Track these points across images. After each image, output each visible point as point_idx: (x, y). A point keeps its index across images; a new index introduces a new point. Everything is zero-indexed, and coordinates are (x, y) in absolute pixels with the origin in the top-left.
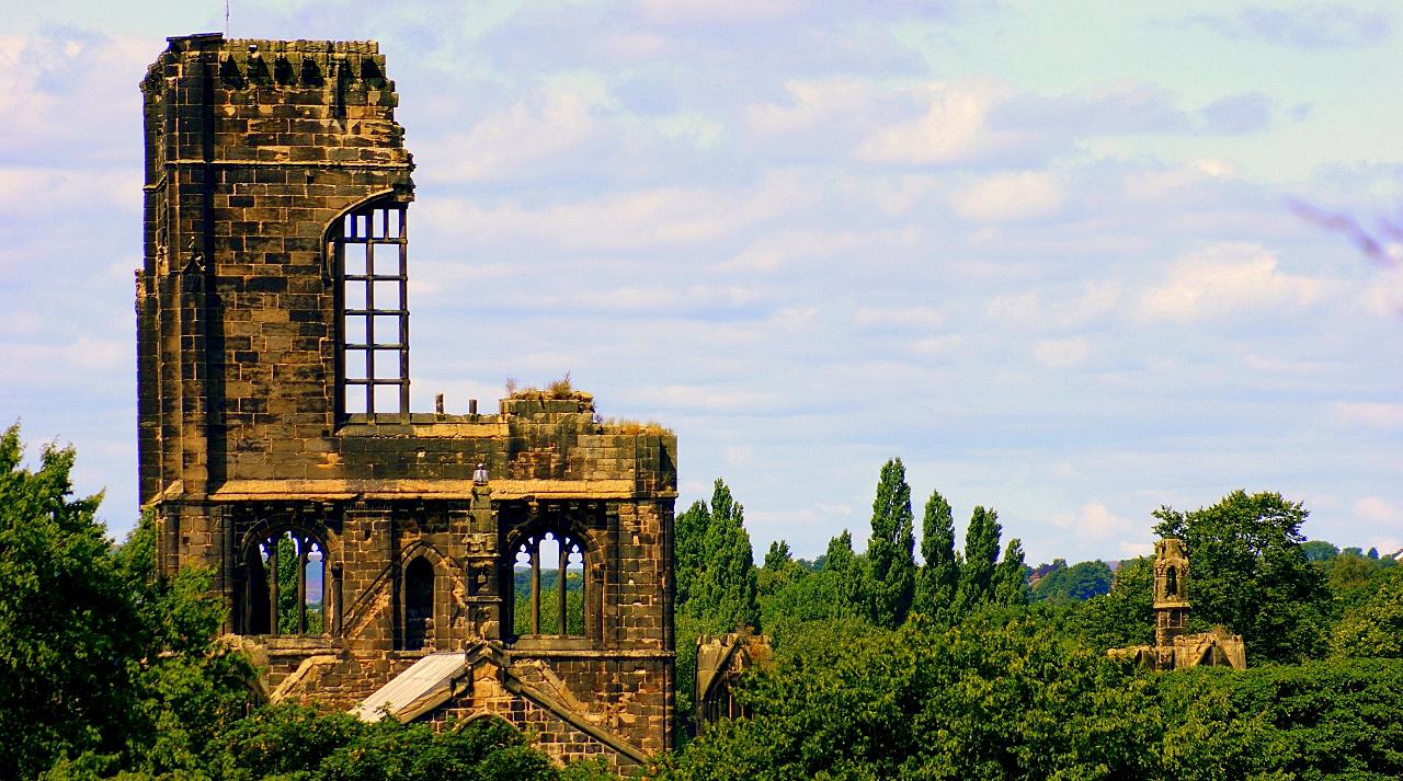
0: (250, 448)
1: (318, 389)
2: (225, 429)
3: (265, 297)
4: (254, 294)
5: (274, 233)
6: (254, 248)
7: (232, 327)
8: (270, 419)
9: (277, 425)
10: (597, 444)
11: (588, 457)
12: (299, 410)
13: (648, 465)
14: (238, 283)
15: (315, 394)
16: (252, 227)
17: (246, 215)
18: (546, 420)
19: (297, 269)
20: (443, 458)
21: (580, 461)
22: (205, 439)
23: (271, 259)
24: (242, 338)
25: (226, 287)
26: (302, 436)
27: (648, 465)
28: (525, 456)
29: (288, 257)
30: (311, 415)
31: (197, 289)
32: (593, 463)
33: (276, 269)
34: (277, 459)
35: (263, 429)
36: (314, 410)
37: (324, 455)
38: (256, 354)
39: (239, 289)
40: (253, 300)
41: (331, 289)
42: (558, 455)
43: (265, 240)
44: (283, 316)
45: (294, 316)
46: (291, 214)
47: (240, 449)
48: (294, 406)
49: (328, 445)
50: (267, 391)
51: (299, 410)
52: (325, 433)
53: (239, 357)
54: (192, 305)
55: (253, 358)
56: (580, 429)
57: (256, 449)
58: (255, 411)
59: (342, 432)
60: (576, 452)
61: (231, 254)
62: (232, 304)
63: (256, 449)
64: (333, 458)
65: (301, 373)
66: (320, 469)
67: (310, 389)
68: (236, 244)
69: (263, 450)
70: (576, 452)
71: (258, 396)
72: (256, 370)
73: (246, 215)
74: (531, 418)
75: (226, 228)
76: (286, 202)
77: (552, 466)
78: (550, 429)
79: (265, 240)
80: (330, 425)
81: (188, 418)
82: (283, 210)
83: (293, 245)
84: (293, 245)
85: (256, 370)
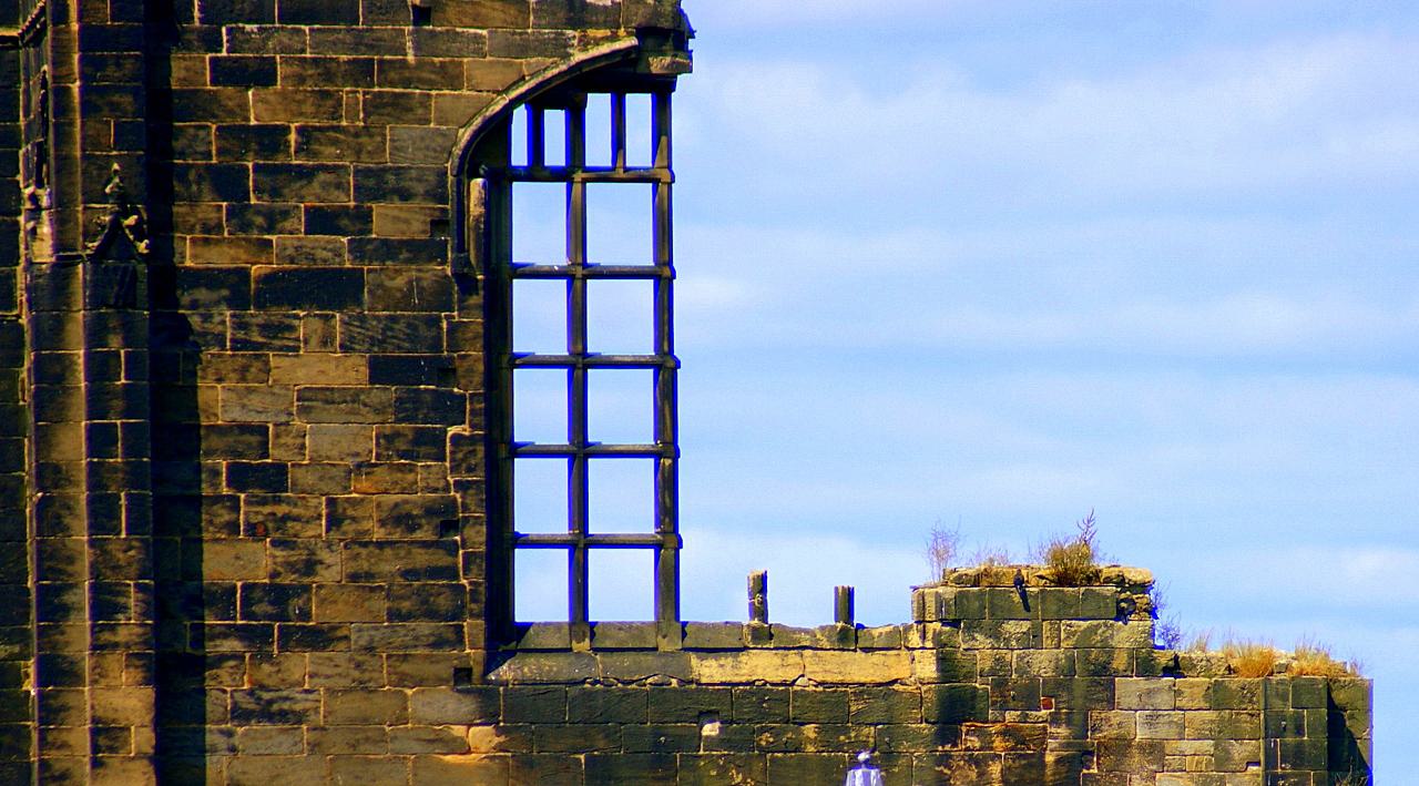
0: (267, 714)
1: (441, 559)
2: (199, 665)
3: (306, 323)
4: (276, 314)
5: (329, 154)
6: (275, 193)
7: (219, 400)
8: (319, 638)
9: (338, 655)
10: (1163, 700)
11: (1141, 734)
12: (394, 615)
13: (1297, 757)
14: (234, 286)
15: (435, 572)
16: (270, 138)
17: (257, 107)
18: (1033, 640)
19: (388, 249)
20: (766, 739)
21: (1121, 746)
22: (149, 693)
23: (321, 221)
24: (245, 428)
25: (202, 294)
26: (403, 680)
27: (1297, 757)
28: (980, 733)
29: (364, 217)
30: (425, 627)
31: (126, 300)
32: (1155, 750)
33: (333, 250)
34: (337, 742)
35: (300, 664)
36: (432, 614)
37: (458, 730)
38: (281, 469)
39: (238, 300)
40: (274, 330)
41: (476, 300)
42: (1063, 731)
43: (305, 174)
44: (350, 371)
45: (381, 371)
46: (375, 106)
47: (240, 715)
48: (380, 605)
49: (468, 706)
50: (310, 566)
51: (394, 615)
52: (462, 675)
53: (239, 476)
54: (115, 342)
55: (274, 479)
56: (1120, 662)
57: (283, 715)
58: (279, 618)
59: (506, 672)
60: (1113, 723)
61: (212, 208)
62: (220, 340)
63: (283, 715)
64: (482, 737)
65: (401, 519)
66: (447, 767)
67: (422, 558)
68: (228, 183)
69: (299, 718)
70: (1113, 723)
71: (288, 579)
72: (281, 510)
73: (257, 107)
74: (995, 634)
75: (204, 142)
76: (362, 72)
77: (1050, 758)
78: (1043, 662)
79: (305, 174)
80: (473, 653)
81: (106, 636)
82: (352, 95)
83: (376, 184)
84: (376, 184)
85: (281, 510)
